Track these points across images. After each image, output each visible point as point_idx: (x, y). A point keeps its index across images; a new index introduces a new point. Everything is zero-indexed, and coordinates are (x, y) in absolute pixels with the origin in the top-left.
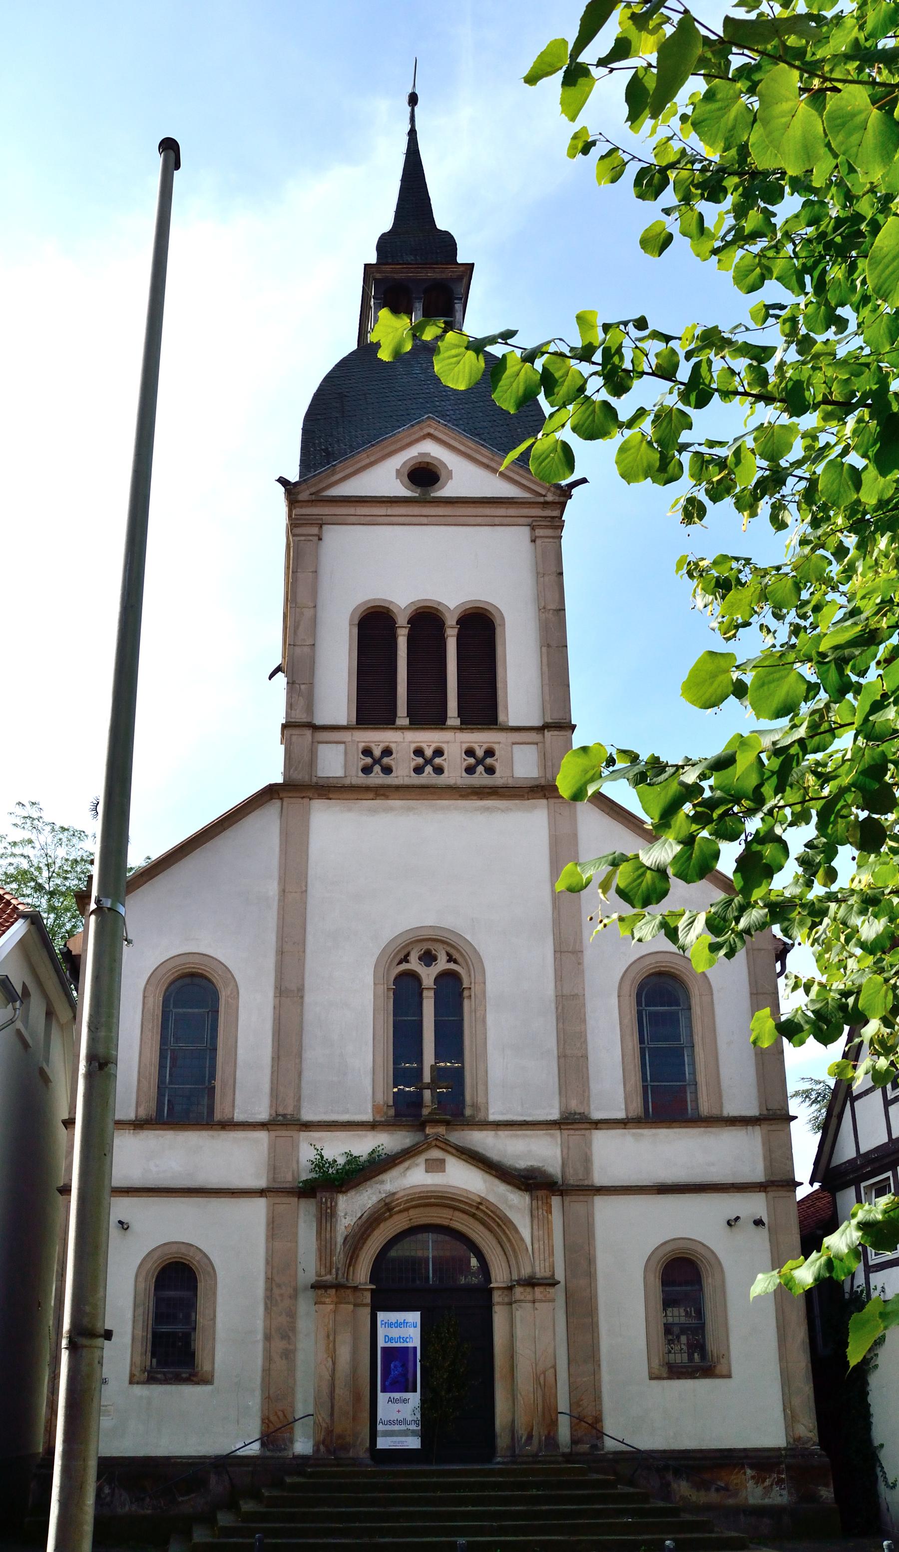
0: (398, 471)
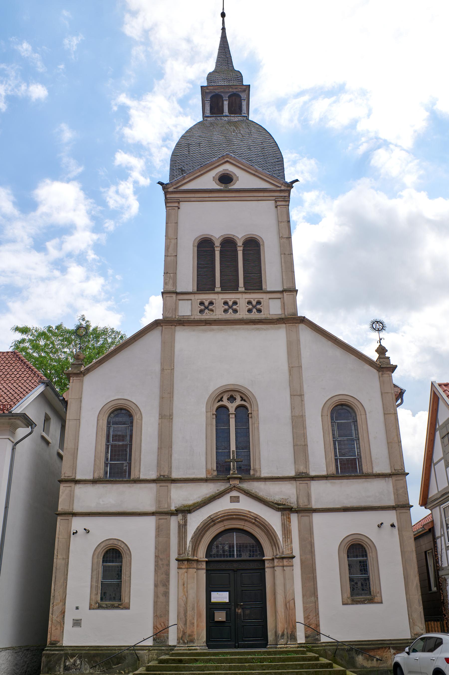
0: (214, 177)
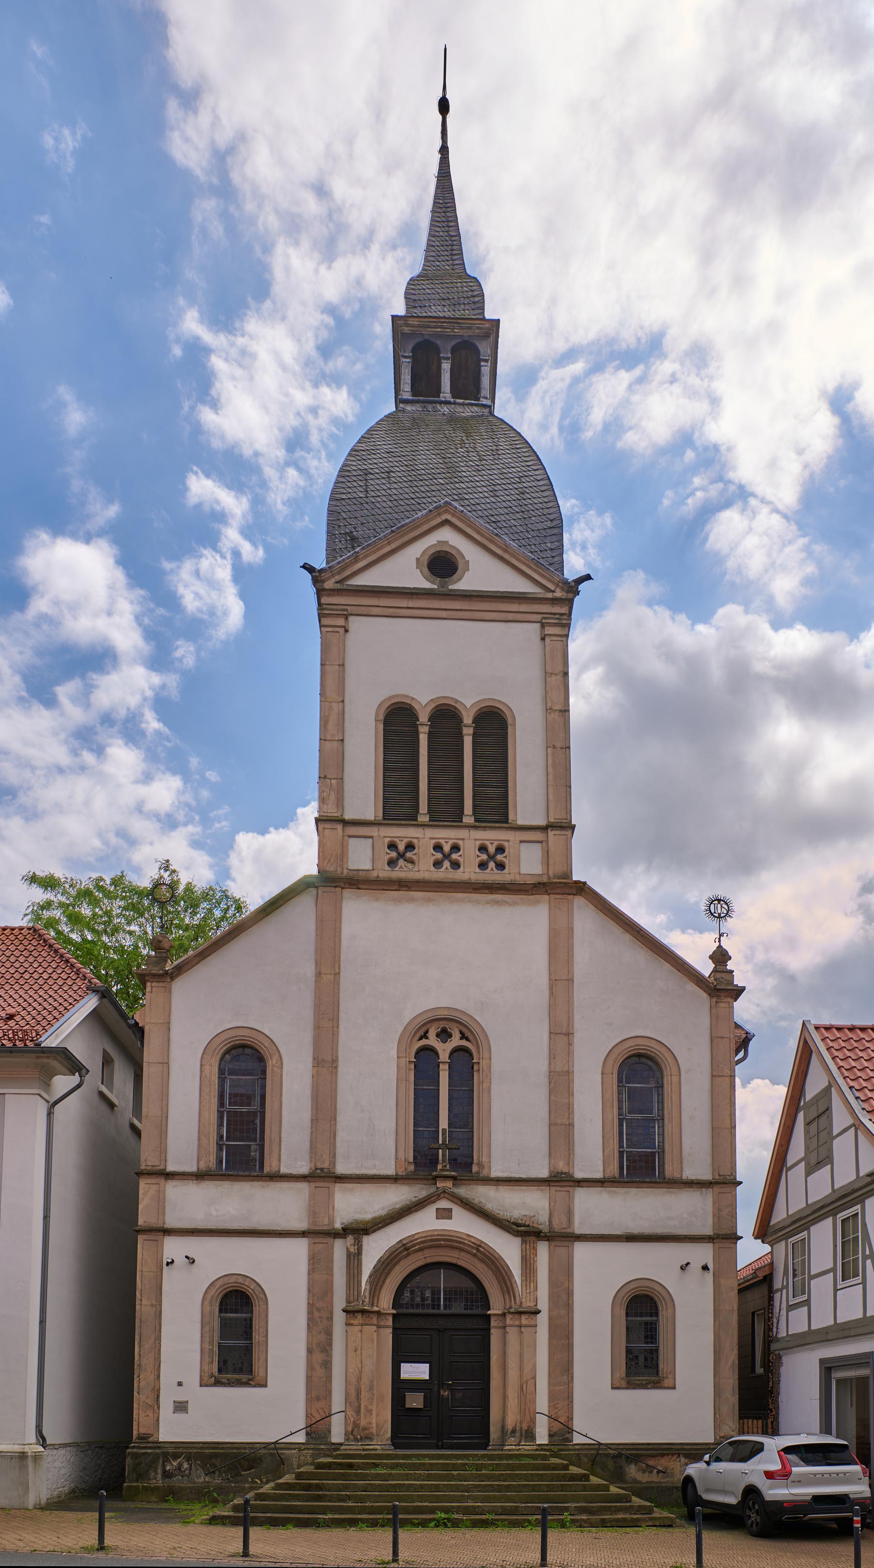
0: (418, 560)
